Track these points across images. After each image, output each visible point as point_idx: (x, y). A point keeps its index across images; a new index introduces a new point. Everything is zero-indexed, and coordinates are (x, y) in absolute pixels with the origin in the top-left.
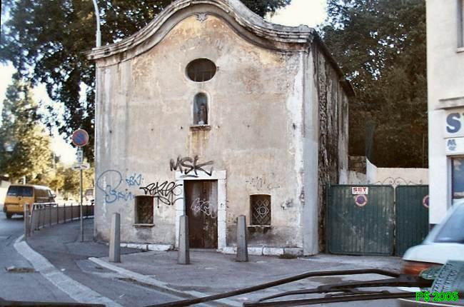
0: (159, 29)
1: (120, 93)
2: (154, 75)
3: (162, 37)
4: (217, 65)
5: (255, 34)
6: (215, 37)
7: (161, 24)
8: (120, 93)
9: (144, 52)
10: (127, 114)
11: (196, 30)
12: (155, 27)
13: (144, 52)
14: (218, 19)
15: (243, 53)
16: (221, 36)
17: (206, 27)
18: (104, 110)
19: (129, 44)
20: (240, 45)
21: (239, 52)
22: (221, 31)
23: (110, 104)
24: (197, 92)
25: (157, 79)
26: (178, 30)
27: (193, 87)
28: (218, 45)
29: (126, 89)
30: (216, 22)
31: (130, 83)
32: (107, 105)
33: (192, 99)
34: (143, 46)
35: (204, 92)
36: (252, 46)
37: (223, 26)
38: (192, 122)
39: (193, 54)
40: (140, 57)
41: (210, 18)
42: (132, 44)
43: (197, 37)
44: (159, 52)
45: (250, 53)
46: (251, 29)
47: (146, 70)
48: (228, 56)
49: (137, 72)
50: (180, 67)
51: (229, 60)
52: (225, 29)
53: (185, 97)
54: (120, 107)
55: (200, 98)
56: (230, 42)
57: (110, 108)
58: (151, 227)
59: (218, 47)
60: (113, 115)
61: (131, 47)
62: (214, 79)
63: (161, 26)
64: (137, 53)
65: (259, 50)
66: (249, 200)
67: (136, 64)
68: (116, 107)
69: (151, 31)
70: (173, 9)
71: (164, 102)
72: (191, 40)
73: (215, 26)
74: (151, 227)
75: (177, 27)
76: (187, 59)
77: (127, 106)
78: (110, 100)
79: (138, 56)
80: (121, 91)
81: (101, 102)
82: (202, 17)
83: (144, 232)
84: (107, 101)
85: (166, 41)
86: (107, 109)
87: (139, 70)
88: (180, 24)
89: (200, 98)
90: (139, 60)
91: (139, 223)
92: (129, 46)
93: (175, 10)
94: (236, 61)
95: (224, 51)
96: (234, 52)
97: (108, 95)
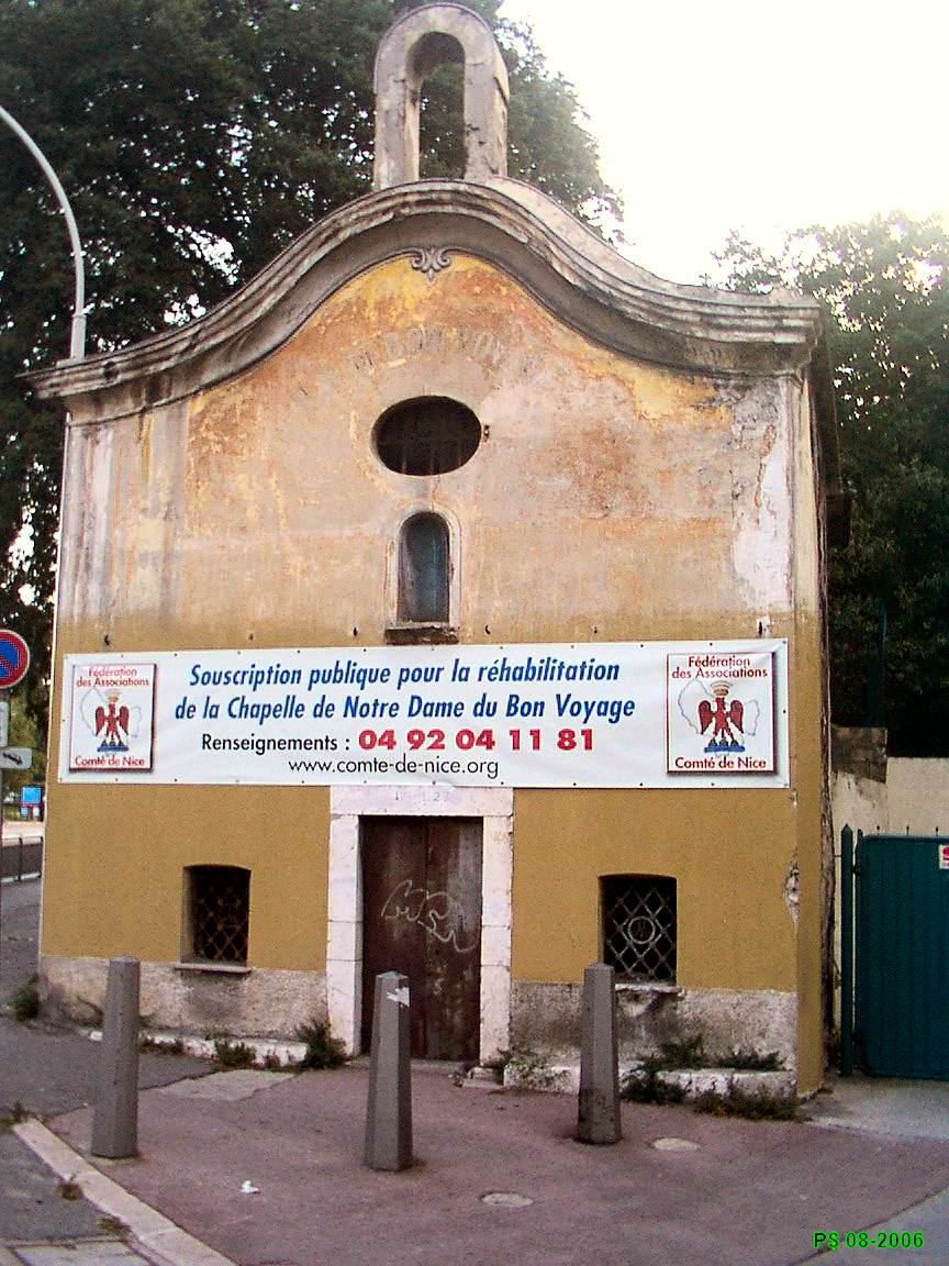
0: (285, 299)
1: (144, 511)
2: (263, 451)
3: (294, 324)
4: (483, 420)
5: (621, 314)
6: (476, 326)
7: (291, 281)
8: (144, 511)
9: (232, 376)
10: (166, 582)
11: (410, 304)
12: (271, 291)
13: (232, 376)
14: (488, 269)
15: (575, 380)
16: (498, 321)
17: (445, 293)
18: (88, 567)
19: (182, 346)
20: (563, 353)
21: (561, 374)
22: (498, 306)
23: (108, 544)
24: (411, 509)
25: (271, 464)
26: (349, 303)
27: (401, 494)
28: (487, 350)
29: (164, 497)
30: (480, 277)
31: (176, 479)
32: (98, 551)
33: (395, 532)
34: (227, 359)
35: (438, 509)
36: (607, 355)
37: (504, 291)
38: (393, 613)
39: (401, 383)
40: (217, 392)
41: (461, 264)
42: (191, 347)
43: (415, 325)
44: (282, 373)
45: (598, 378)
46: (609, 296)
47: (233, 435)
48: (520, 388)
49: (206, 441)
50: (353, 425)
51: (526, 403)
52: (513, 300)
53: (370, 528)
54: (144, 557)
55: (425, 534)
56: (530, 340)
57: (108, 560)
58: (239, 976)
59: (489, 358)
60: (116, 583)
61: (187, 357)
62: (472, 465)
63: (292, 290)
64: (209, 376)
65: (627, 369)
66: (476, 814)
67: (203, 414)
68: (131, 559)
69: (259, 302)
70: (337, 232)
71: (296, 542)
72: (395, 336)
73: (477, 289)
74: (239, 976)
75: (345, 295)
76: (377, 399)
77: (168, 556)
78: (109, 532)
79: (209, 387)
80: (148, 504)
81: (80, 540)
82: (432, 259)
83: (216, 993)
84: (101, 535)
85: (307, 338)
86: (97, 563)
87: (211, 436)
88: (356, 284)
89: (425, 534)
90: (212, 403)
91: (210, 955)
92: (182, 353)
93: (343, 235)
94: (550, 406)
95: (508, 372)
96: (545, 377)
97: (102, 516)
